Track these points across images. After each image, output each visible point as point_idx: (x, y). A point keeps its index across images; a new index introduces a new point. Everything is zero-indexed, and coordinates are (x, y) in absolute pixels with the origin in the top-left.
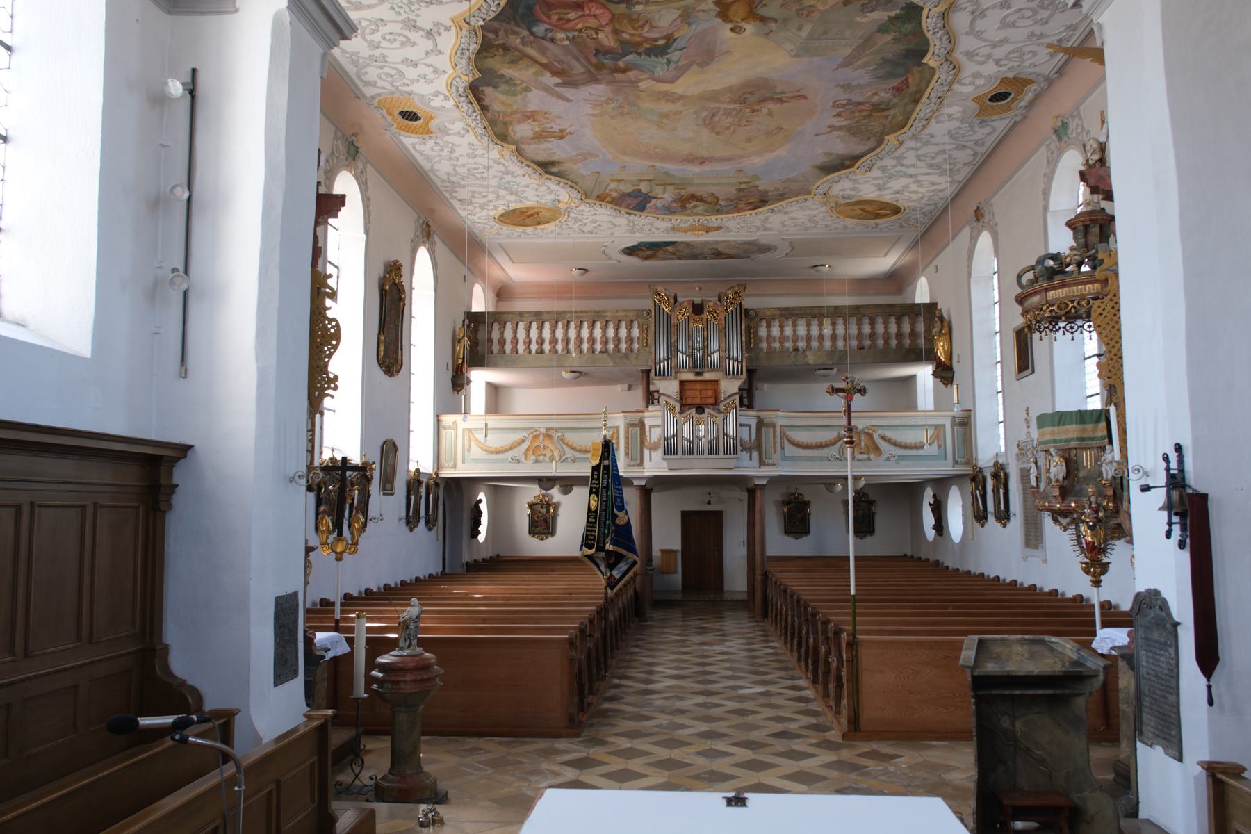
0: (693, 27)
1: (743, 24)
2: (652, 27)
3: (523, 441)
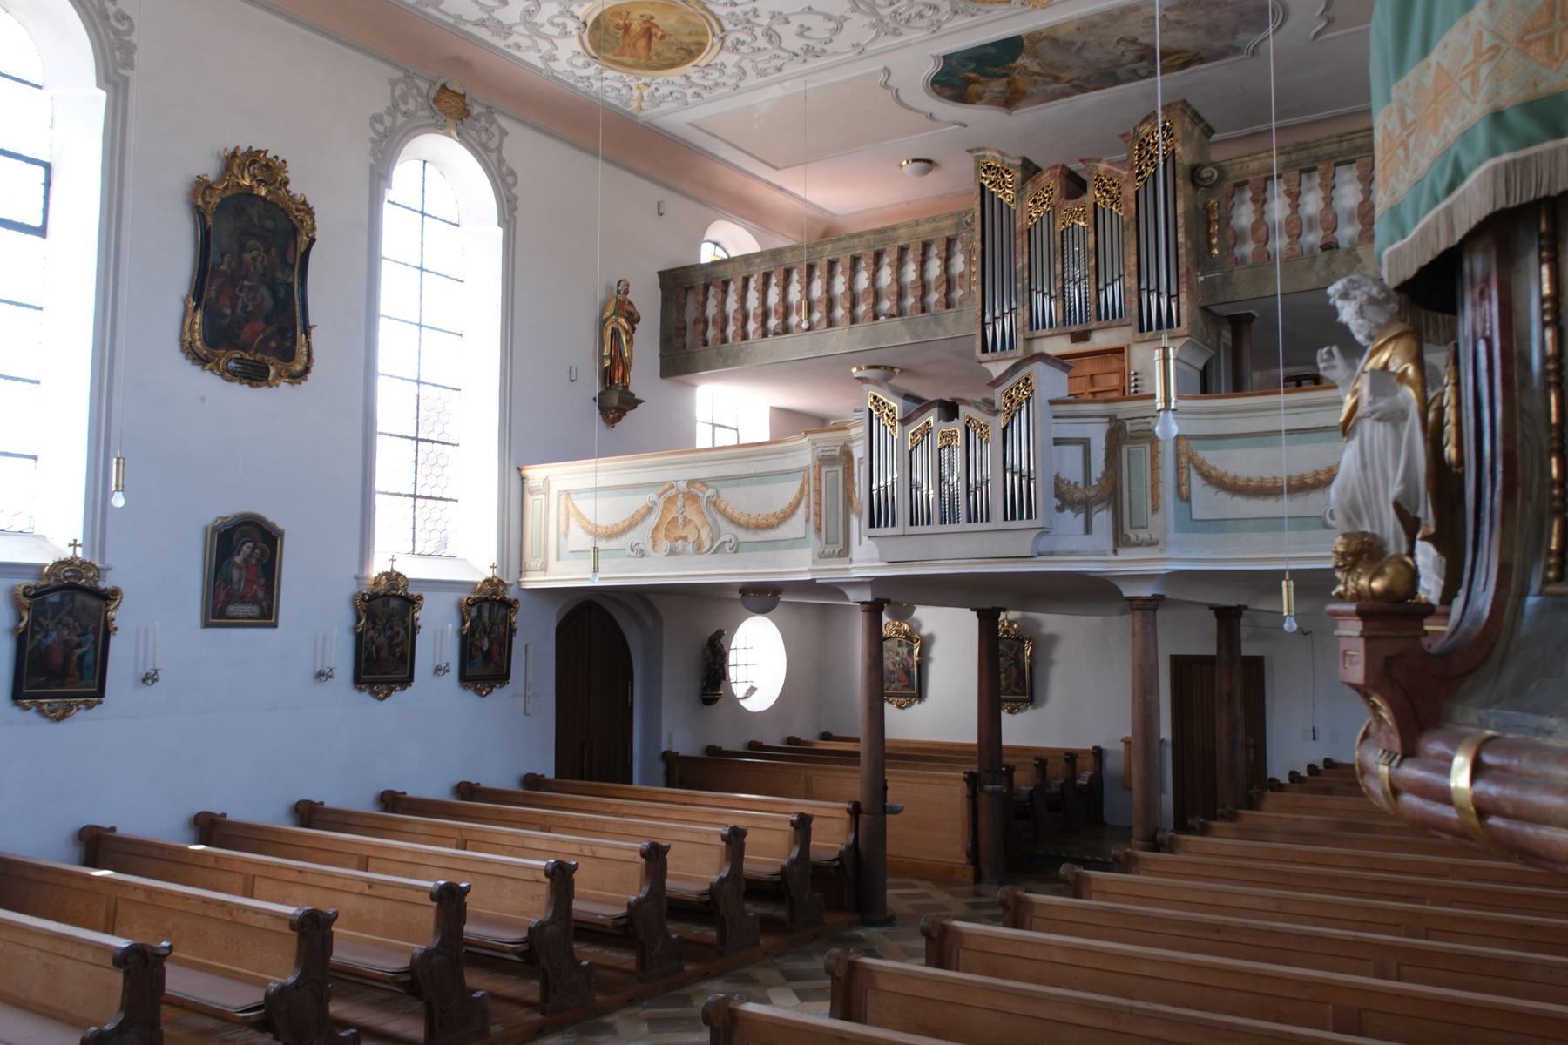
3: (650, 510)
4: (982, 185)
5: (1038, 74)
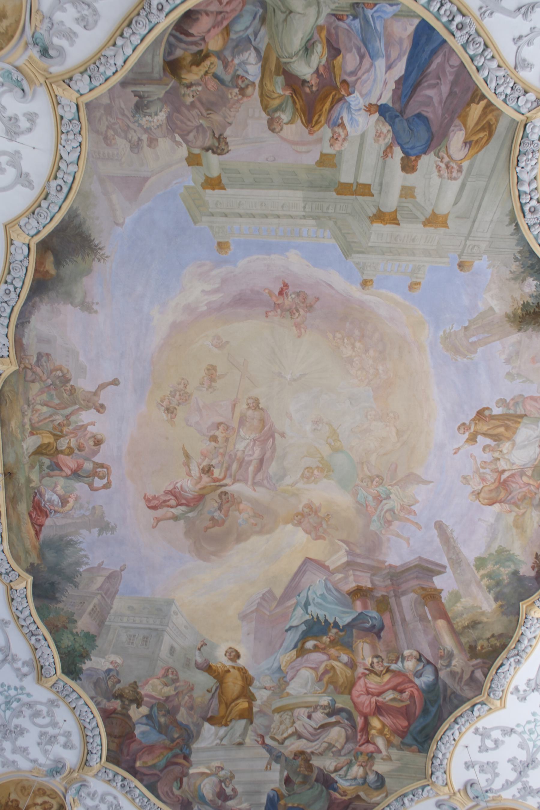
0: (276, 665)
1: (228, 664)
2: (315, 669)
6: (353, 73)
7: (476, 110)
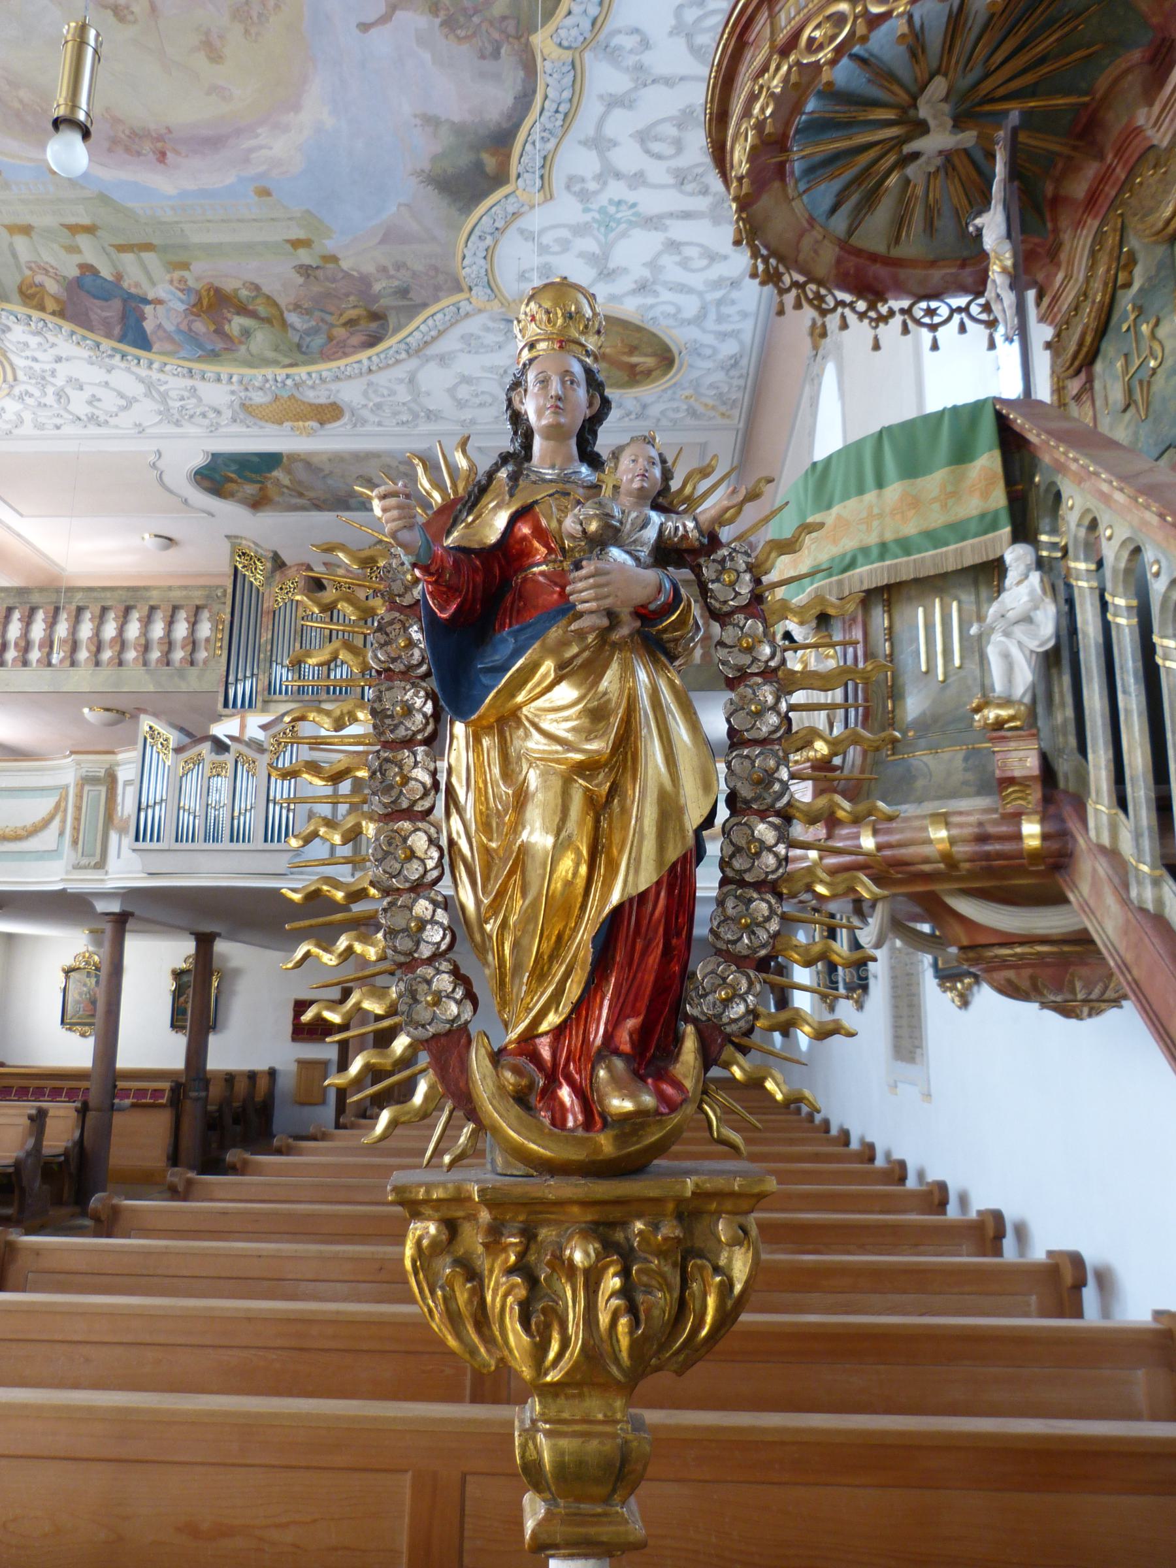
4: (236, 568)
5: (287, 488)
6: (193, 321)
7: (51, 305)
